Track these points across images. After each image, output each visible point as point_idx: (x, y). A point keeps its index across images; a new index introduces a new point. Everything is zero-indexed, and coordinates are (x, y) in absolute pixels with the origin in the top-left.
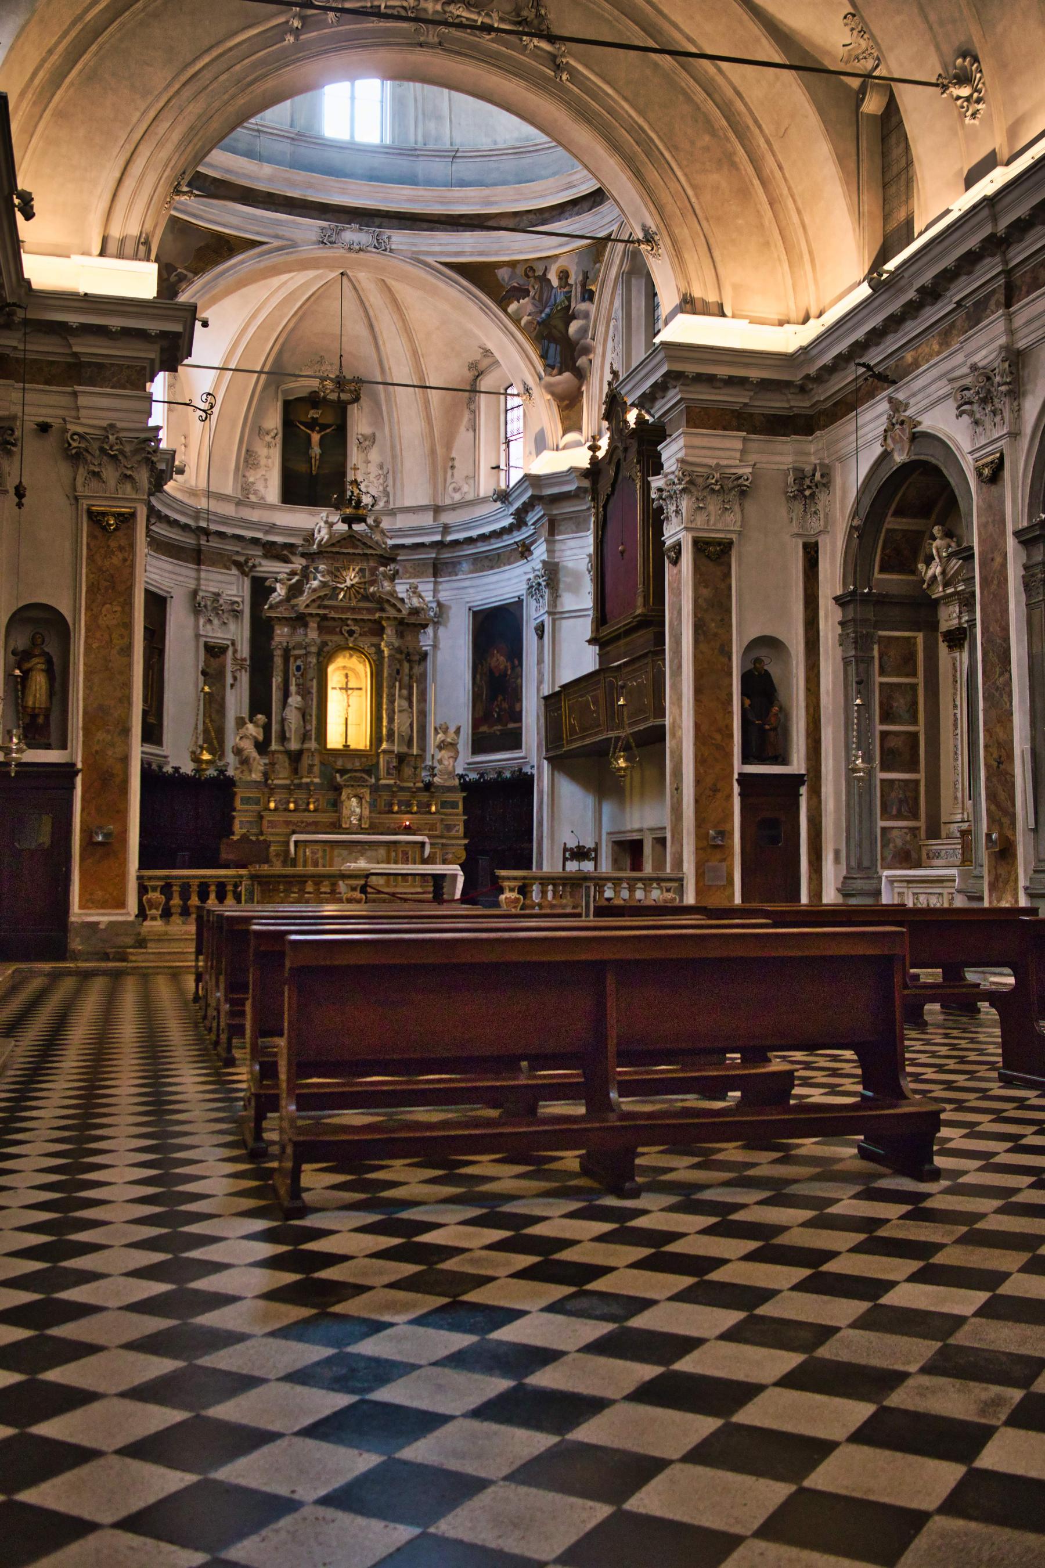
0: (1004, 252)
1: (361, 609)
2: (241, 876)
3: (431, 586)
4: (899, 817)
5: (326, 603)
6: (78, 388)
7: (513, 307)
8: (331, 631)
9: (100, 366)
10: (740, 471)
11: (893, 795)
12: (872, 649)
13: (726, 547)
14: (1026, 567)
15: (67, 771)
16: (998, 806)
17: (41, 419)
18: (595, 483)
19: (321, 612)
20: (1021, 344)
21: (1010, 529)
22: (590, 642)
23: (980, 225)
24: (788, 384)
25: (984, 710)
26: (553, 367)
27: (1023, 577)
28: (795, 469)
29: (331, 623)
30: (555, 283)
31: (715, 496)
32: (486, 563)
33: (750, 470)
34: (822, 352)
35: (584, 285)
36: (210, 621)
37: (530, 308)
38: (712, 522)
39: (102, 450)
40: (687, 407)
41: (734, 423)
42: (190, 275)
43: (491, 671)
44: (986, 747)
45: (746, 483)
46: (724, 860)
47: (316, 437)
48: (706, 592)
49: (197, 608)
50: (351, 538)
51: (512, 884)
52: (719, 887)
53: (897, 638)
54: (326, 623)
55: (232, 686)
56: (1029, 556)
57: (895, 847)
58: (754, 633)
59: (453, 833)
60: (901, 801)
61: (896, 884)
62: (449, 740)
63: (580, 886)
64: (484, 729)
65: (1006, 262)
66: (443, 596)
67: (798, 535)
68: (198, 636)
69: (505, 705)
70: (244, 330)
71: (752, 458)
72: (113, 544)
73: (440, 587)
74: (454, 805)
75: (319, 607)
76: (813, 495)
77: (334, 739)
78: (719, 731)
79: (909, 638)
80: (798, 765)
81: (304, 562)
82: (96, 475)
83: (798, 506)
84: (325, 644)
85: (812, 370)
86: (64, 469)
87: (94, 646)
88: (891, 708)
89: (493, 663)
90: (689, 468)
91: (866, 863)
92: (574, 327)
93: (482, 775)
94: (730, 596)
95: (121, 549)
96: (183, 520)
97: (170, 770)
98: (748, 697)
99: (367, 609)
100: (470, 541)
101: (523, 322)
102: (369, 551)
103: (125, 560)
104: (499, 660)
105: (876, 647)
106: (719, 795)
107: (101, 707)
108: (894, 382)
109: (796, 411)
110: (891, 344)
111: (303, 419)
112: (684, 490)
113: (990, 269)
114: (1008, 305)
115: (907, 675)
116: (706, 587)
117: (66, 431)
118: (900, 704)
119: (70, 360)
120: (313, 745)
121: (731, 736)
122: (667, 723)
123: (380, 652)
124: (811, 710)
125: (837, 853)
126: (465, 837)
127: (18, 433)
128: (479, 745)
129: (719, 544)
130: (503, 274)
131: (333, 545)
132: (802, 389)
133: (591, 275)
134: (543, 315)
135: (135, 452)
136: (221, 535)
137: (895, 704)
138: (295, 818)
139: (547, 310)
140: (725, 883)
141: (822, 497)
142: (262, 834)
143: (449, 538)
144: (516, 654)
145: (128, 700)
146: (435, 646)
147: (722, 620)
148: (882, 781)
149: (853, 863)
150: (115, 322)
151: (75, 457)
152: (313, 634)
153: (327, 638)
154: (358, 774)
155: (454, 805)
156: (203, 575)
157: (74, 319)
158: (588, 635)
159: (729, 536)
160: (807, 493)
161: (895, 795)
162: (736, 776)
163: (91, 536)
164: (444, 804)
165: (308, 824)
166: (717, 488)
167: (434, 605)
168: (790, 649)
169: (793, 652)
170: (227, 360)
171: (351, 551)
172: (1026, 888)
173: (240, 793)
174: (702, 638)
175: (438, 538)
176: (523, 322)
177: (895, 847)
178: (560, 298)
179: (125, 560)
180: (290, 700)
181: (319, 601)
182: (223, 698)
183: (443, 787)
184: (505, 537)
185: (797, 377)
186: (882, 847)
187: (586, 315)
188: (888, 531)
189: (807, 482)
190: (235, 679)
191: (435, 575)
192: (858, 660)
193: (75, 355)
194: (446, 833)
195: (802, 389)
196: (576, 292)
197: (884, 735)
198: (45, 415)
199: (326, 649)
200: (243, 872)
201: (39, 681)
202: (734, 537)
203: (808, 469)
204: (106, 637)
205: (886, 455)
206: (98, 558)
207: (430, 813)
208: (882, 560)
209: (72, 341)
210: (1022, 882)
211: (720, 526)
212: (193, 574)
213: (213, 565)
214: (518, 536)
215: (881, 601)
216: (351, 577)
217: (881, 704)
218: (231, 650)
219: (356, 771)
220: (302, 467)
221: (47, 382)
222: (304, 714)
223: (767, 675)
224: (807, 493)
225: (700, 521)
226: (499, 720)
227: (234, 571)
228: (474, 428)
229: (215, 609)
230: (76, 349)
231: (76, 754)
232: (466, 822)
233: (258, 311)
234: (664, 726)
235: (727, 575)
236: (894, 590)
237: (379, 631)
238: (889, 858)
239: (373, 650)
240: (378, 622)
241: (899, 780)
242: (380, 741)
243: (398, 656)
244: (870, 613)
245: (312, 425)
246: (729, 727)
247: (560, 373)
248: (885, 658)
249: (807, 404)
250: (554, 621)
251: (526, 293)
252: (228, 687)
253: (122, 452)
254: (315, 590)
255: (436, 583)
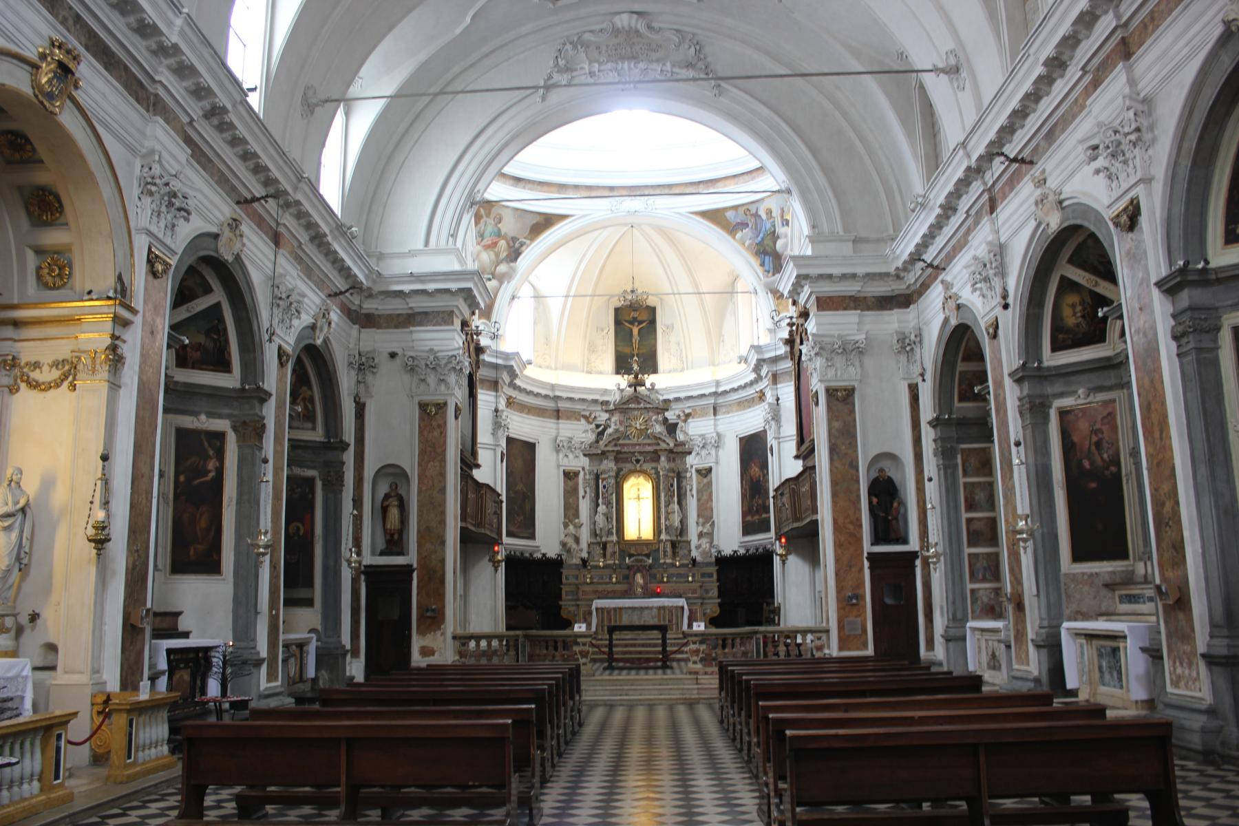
0: (983, 177)
1: (644, 444)
2: (518, 636)
3: (712, 422)
4: (984, 580)
5: (621, 442)
6: (412, 329)
7: (739, 235)
8: (626, 460)
9: (426, 313)
10: (857, 338)
11: (979, 565)
12: (956, 458)
13: (850, 392)
14: (1020, 399)
15: (408, 569)
16: (1016, 578)
17: (390, 350)
18: (792, 348)
19: (616, 449)
20: (1003, 240)
21: (1006, 372)
22: (797, 457)
23: (960, 162)
24: (887, 275)
25: (1005, 506)
26: (769, 272)
27: (1019, 407)
28: (897, 333)
29: (625, 456)
30: (764, 216)
31: (840, 357)
32: (746, 404)
33: (864, 336)
34: (902, 252)
35: (782, 216)
36: (566, 456)
37: (750, 235)
38: (839, 374)
39: (427, 365)
40: (817, 298)
41: (852, 304)
42: (528, 242)
43: (751, 478)
44: (1006, 533)
45: (862, 346)
46: (859, 616)
47: (635, 331)
48: (837, 425)
49: (558, 449)
50: (636, 398)
51: (694, 639)
52: (855, 636)
53: (975, 449)
54: (621, 456)
55: (583, 497)
56: (1021, 391)
57: (982, 603)
58: (874, 452)
59: (710, 594)
60: (985, 569)
61: (976, 632)
62: (705, 531)
63: (752, 638)
64: (749, 518)
65: (985, 183)
66: (720, 429)
67: (904, 379)
68: (559, 466)
69: (760, 502)
70: (577, 268)
71: (867, 327)
72: (434, 424)
73: (719, 423)
74: (710, 575)
75: (616, 445)
76: (912, 349)
77: (631, 533)
78: (851, 522)
79: (984, 449)
80: (914, 544)
81: (606, 416)
82: (424, 380)
83: (903, 358)
84: (619, 470)
85: (900, 264)
86: (406, 378)
87: (424, 488)
88: (974, 500)
89: (752, 472)
90: (819, 339)
91: (959, 616)
92: (779, 244)
93: (748, 551)
94: (855, 426)
95: (439, 426)
96: (543, 392)
97: (540, 556)
98: (876, 496)
99: (649, 445)
100: (734, 390)
101: (746, 244)
102: (648, 406)
103: (441, 433)
104: (755, 470)
105: (959, 457)
106: (853, 569)
107: (427, 527)
108: (944, 269)
109: (897, 292)
110: (940, 242)
111: (627, 318)
112: (816, 354)
113: (976, 188)
114: (992, 213)
115: (985, 475)
116: (837, 420)
117: (405, 355)
118: (980, 496)
119: (410, 312)
120: (614, 538)
121: (861, 526)
122: (819, 518)
123: (657, 473)
124: (921, 504)
125: (942, 608)
126: (719, 597)
127: (376, 360)
128: (748, 529)
129: (845, 390)
130: (730, 215)
131: (624, 403)
132: (898, 277)
133: (785, 209)
134: (759, 239)
135: (446, 364)
136: (571, 399)
137: (977, 498)
138: (600, 588)
139: (761, 235)
140: (859, 632)
141: (917, 350)
142: (578, 600)
143: (721, 389)
144: (764, 466)
145: (443, 522)
146: (717, 463)
147: (850, 444)
148: (970, 555)
149: (951, 617)
150: (431, 287)
151: (411, 369)
152: (609, 465)
153: (621, 465)
154: (640, 558)
155: (710, 575)
156: (561, 426)
157: (407, 288)
158: (794, 452)
159: (852, 383)
160: (908, 348)
161: (981, 564)
162: (865, 555)
163: (421, 419)
164: (703, 575)
165: (609, 592)
166: (840, 351)
167: (714, 435)
168: (903, 459)
169: (906, 463)
170: (569, 290)
171: (636, 406)
172: (1032, 640)
173: (565, 572)
174: (835, 457)
175: (713, 390)
176: (746, 244)
177: (982, 603)
178: (768, 226)
179: (441, 433)
180: (599, 509)
181: (615, 440)
182: (578, 506)
183: (703, 563)
184: (748, 389)
185: (891, 269)
186: (972, 603)
187: (786, 236)
188: (961, 373)
189: (907, 341)
190: (585, 492)
191: (715, 414)
192: (946, 468)
193: (411, 308)
194: (705, 595)
195: (898, 277)
196: (778, 222)
197: (969, 521)
198: (394, 347)
199: (621, 473)
200: (519, 632)
201: (394, 512)
202: (856, 385)
203: (907, 332)
204: (431, 482)
205: (946, 320)
206: (425, 433)
207: (688, 581)
208: (960, 393)
209: (408, 300)
210: (1031, 635)
211: (845, 377)
212: (554, 426)
213: (568, 418)
214: (759, 387)
215: (961, 423)
216: (638, 424)
217: (966, 500)
218: (581, 475)
219: (639, 555)
220: (627, 350)
221: (396, 327)
222: (607, 517)
223: (890, 480)
224: (908, 348)
225: (831, 374)
226: (757, 512)
227: (583, 421)
228: (735, 314)
229: (569, 448)
230: (411, 305)
231: (411, 558)
232: (719, 587)
233: (584, 256)
234: (817, 520)
235: (852, 411)
236: (970, 415)
237: (657, 460)
238: (978, 611)
239: (653, 471)
240: (656, 452)
241: (983, 554)
242: (659, 536)
243: (672, 474)
244: (953, 432)
245: (632, 323)
246: (859, 519)
247: (774, 275)
248: (967, 464)
249: (904, 287)
250: (779, 443)
251: (747, 225)
252: (581, 498)
253: (439, 365)
254: (610, 435)
255: (715, 420)
